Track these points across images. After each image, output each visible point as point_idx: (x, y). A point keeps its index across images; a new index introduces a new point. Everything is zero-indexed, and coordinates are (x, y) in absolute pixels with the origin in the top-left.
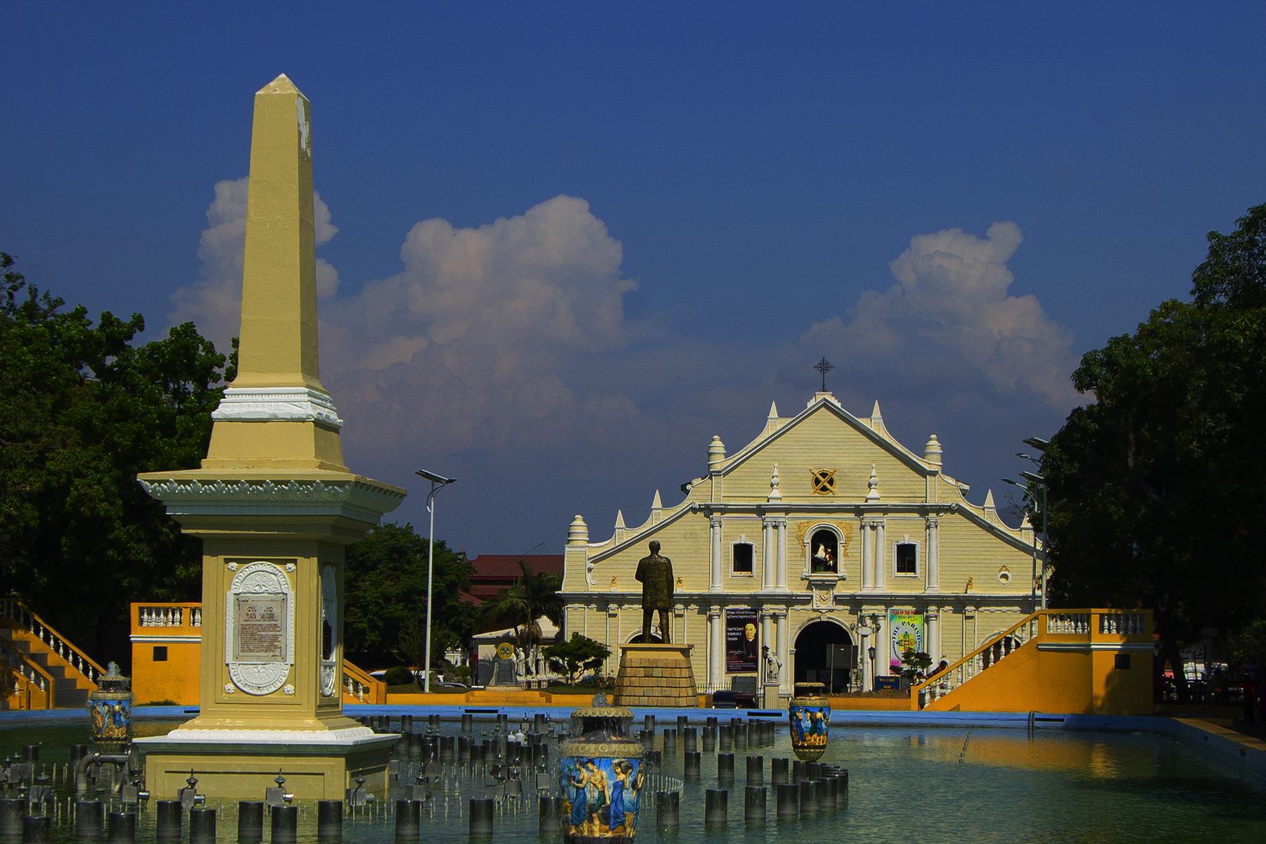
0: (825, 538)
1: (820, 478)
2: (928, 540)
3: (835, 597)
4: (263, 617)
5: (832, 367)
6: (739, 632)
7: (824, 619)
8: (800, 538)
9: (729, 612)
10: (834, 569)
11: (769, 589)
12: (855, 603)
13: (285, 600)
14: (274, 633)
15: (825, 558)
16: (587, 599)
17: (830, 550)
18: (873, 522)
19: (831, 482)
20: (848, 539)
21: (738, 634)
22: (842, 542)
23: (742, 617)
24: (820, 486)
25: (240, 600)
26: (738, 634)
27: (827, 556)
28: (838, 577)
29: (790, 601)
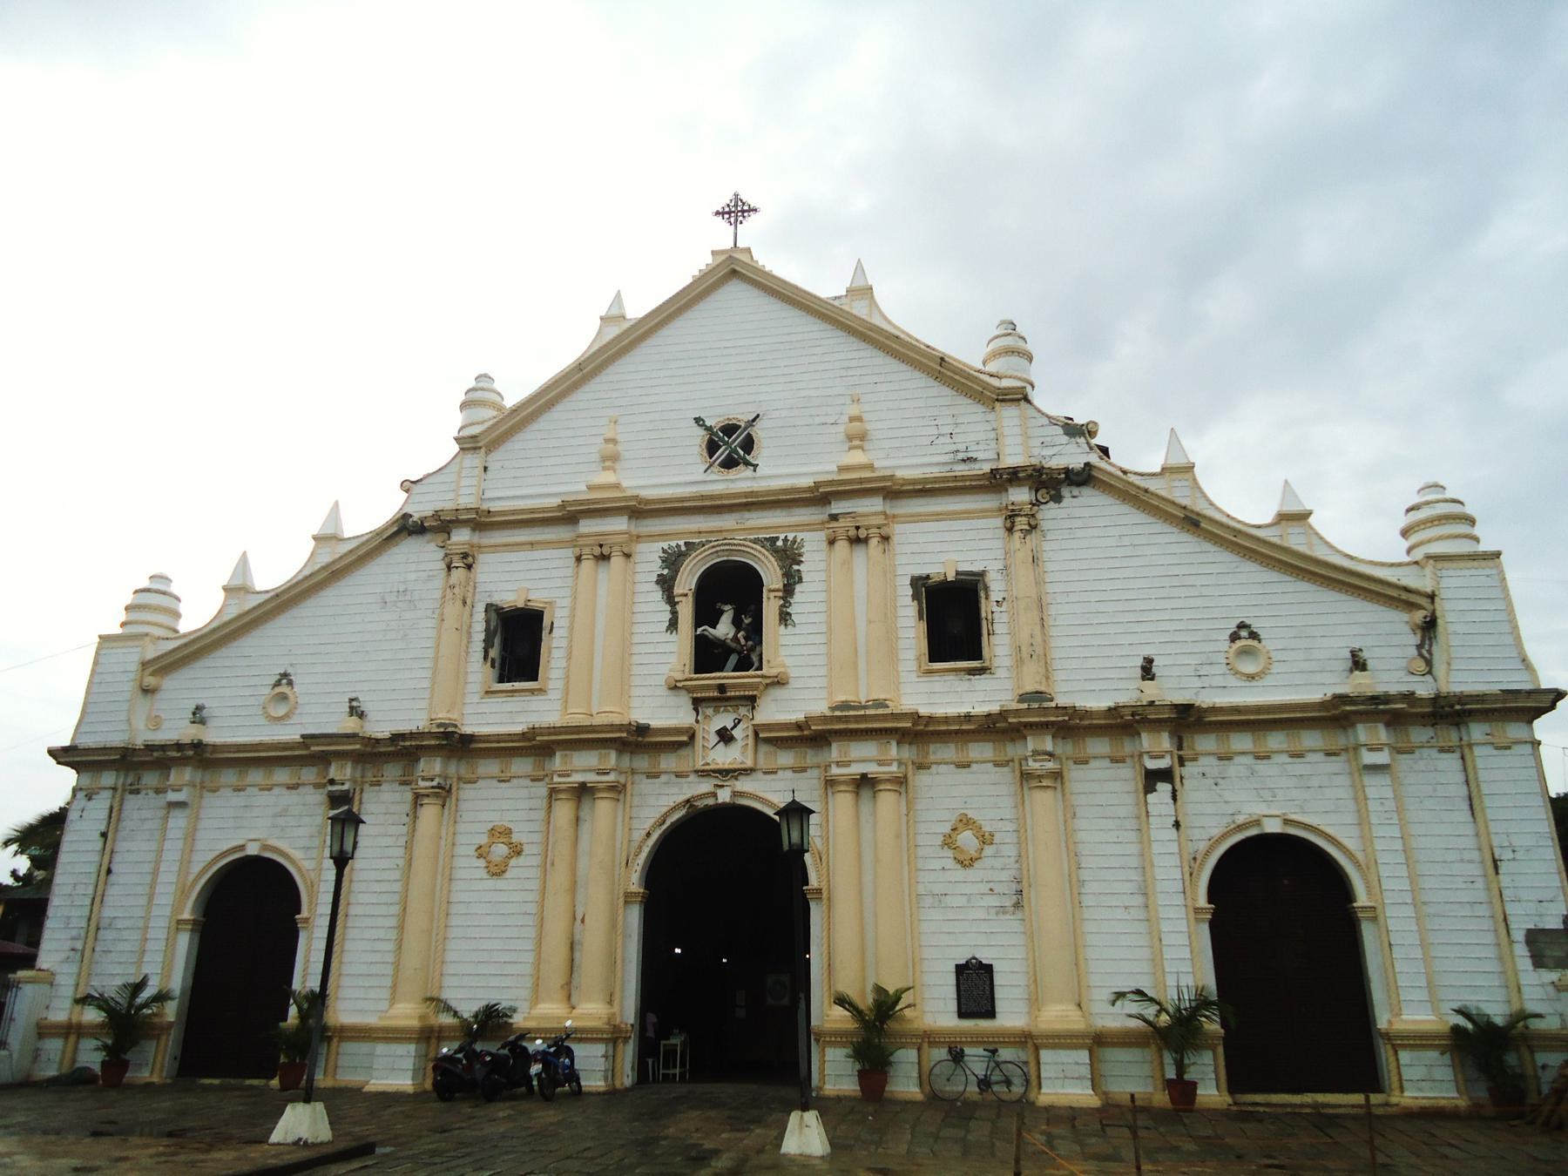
5: (756, 210)
7: (724, 796)
8: (666, 584)
15: (735, 638)
17: (747, 621)
18: (858, 528)
22: (773, 587)
28: (763, 677)
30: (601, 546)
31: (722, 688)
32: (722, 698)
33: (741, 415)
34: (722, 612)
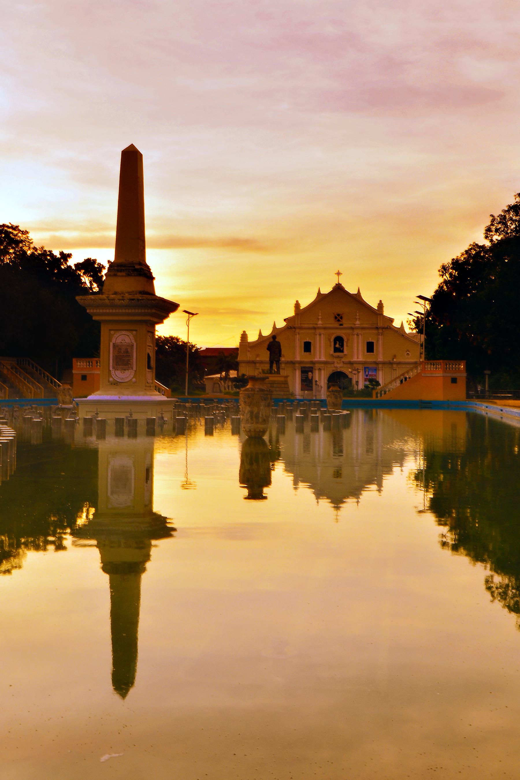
0: (339, 340)
1: (337, 316)
2: (378, 341)
3: (343, 362)
4: (124, 352)
6: (306, 375)
8: (329, 340)
9: (302, 368)
10: (342, 351)
11: (317, 359)
12: (351, 363)
13: (133, 345)
14: (128, 358)
16: (248, 362)
19: (341, 318)
20: (348, 340)
21: (305, 376)
22: (346, 341)
23: (307, 370)
24: (337, 319)
25: (114, 346)
26: (305, 376)
27: (340, 346)
29: (326, 363)
30: (320, 333)
31: (338, 356)
32: (338, 357)
33: (340, 313)
34: (337, 343)
